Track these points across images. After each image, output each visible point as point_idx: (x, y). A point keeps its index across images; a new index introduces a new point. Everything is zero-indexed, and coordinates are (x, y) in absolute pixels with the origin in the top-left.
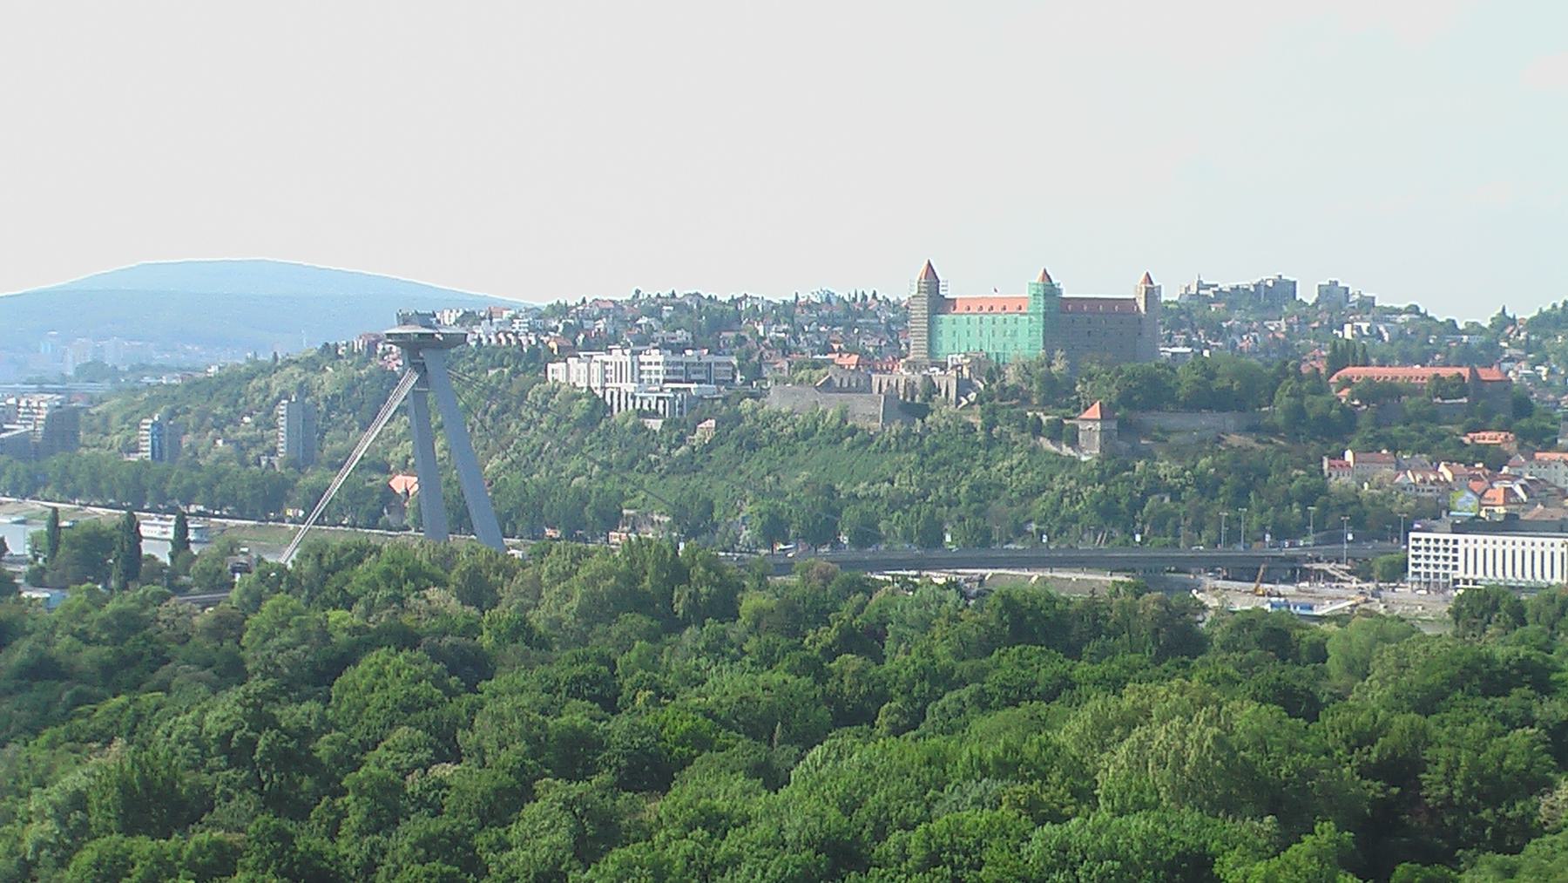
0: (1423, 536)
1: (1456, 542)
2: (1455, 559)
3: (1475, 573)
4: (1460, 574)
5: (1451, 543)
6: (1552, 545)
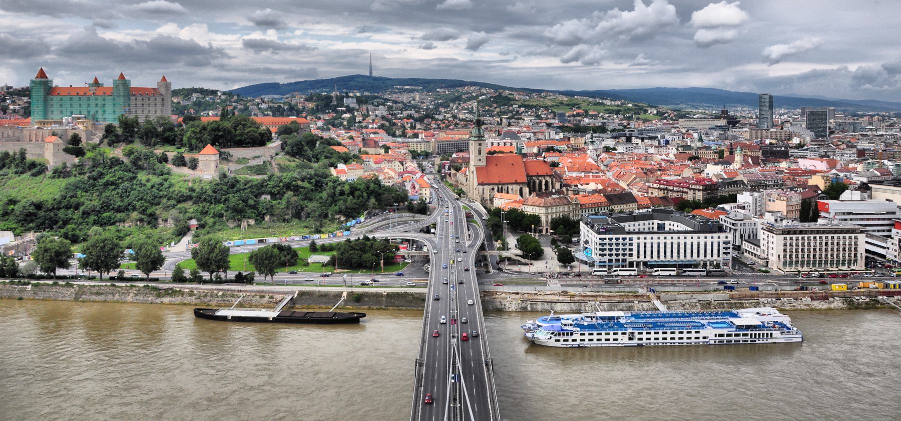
0: (607, 236)
1: (630, 239)
2: (631, 250)
3: (645, 257)
4: (634, 258)
5: (627, 241)
6: (699, 238)
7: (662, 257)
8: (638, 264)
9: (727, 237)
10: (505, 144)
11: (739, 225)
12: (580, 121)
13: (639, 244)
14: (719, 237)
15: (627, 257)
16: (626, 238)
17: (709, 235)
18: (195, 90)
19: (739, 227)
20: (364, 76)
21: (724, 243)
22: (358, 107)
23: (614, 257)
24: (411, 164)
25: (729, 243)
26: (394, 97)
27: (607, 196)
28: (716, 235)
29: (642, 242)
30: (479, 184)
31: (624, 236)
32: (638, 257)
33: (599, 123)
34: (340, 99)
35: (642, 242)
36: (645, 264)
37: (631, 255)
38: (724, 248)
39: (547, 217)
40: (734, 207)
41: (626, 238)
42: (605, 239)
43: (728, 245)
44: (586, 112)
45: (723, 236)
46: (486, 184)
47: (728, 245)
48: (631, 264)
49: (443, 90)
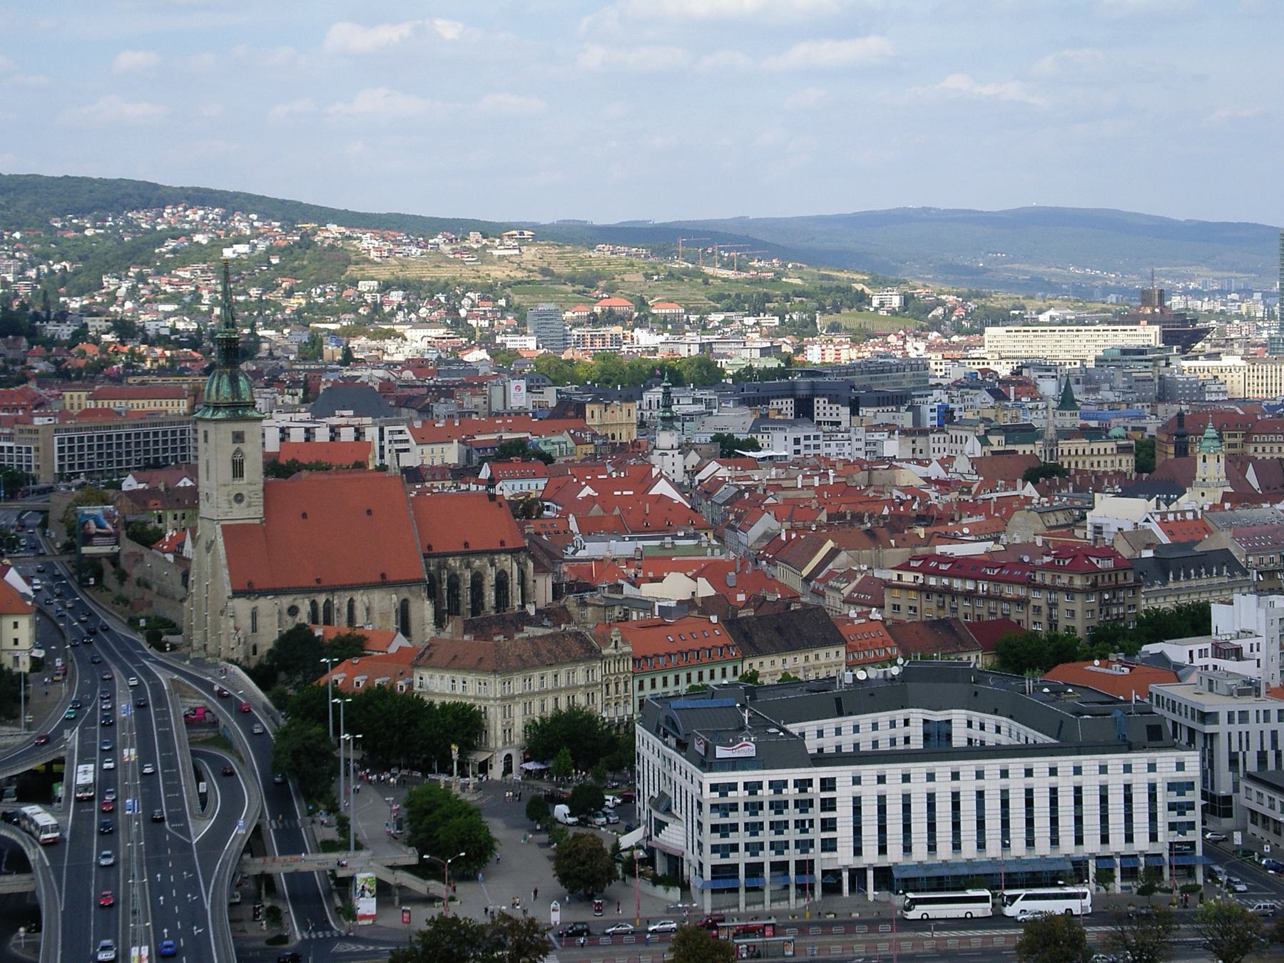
1: (828, 784)
2: (829, 825)
3: (883, 850)
4: (844, 857)
5: (815, 791)
6: (1078, 771)
7: (944, 851)
8: (858, 876)
9: (1180, 766)
11: (1223, 718)
12: (617, 340)
13: (857, 802)
14: (1152, 767)
15: (815, 854)
16: (809, 782)
17: (1114, 761)
19: (1222, 728)
21: (1171, 786)
23: (767, 857)
25: (1190, 786)
27: (731, 623)
28: (1139, 760)
29: (869, 792)
30: (237, 594)
31: (802, 773)
32: (858, 851)
33: (689, 346)
35: (869, 792)
36: (885, 877)
37: (829, 846)
38: (1172, 807)
39: (507, 713)
40: (1202, 653)
41: (809, 782)
42: (733, 787)
43: (1189, 797)
44: (642, 304)
45: (1166, 761)
46: (264, 593)
47: (1189, 797)
48: (832, 881)
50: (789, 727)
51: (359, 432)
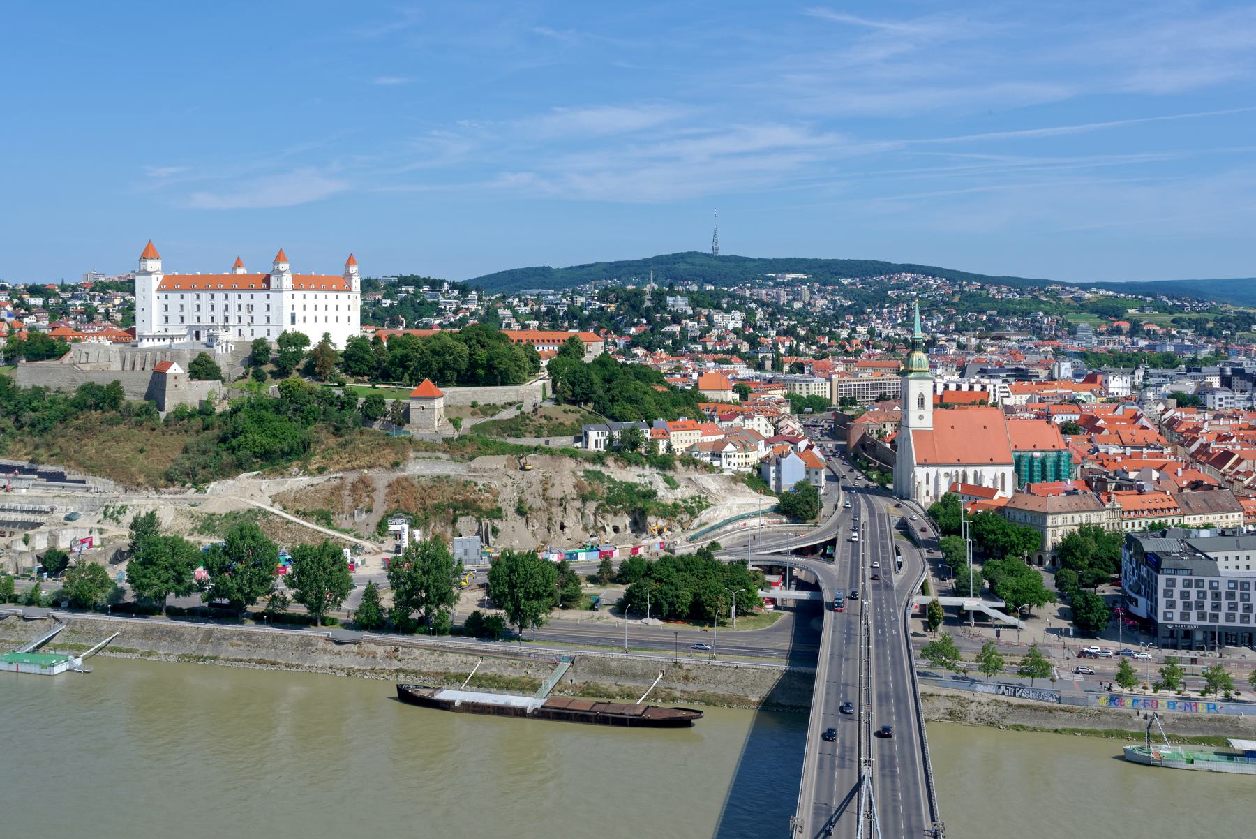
10: (971, 387)
18: (404, 281)
20: (705, 254)
22: (690, 312)
24: (790, 423)
26: (764, 294)
30: (919, 464)
34: (659, 297)
49: (850, 280)
50: (1208, 554)
51: (984, 388)
